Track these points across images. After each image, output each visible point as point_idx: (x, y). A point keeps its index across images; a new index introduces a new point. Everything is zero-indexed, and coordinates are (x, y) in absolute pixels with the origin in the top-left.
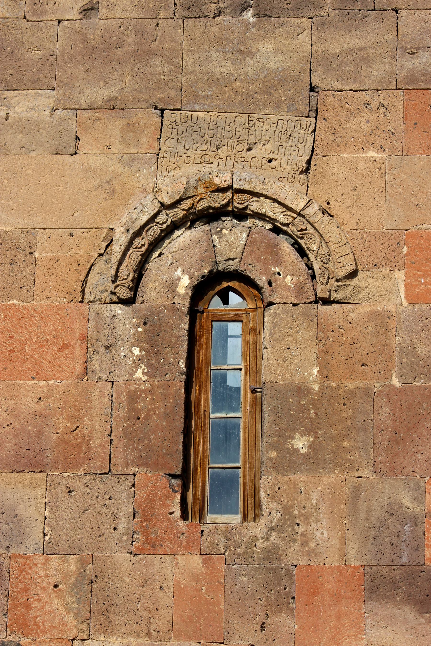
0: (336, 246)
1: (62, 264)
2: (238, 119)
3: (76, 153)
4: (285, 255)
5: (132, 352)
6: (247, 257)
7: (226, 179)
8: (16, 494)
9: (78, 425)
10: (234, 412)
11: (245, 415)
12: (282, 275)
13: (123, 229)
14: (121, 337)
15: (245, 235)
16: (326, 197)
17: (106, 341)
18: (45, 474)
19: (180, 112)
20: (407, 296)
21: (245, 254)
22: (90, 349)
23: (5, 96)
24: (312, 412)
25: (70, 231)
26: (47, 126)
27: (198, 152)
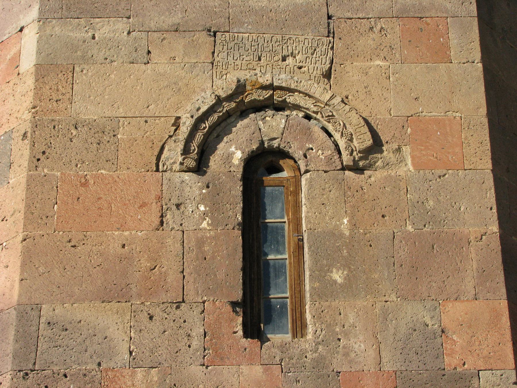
0: (357, 127)
1: (140, 143)
2: (274, 39)
3: (148, 63)
4: (316, 135)
5: (198, 208)
6: (286, 137)
7: (268, 79)
8: (106, 320)
9: (156, 265)
10: (281, 254)
11: (290, 256)
12: (314, 151)
13: (189, 115)
14: (189, 197)
15: (283, 121)
16: (345, 94)
17: (177, 200)
18: (130, 304)
19: (228, 34)
20: (413, 164)
21: (284, 135)
22: (164, 207)
23: (91, 22)
24: (345, 251)
25: (144, 119)
26: (125, 43)
27: (244, 62)
